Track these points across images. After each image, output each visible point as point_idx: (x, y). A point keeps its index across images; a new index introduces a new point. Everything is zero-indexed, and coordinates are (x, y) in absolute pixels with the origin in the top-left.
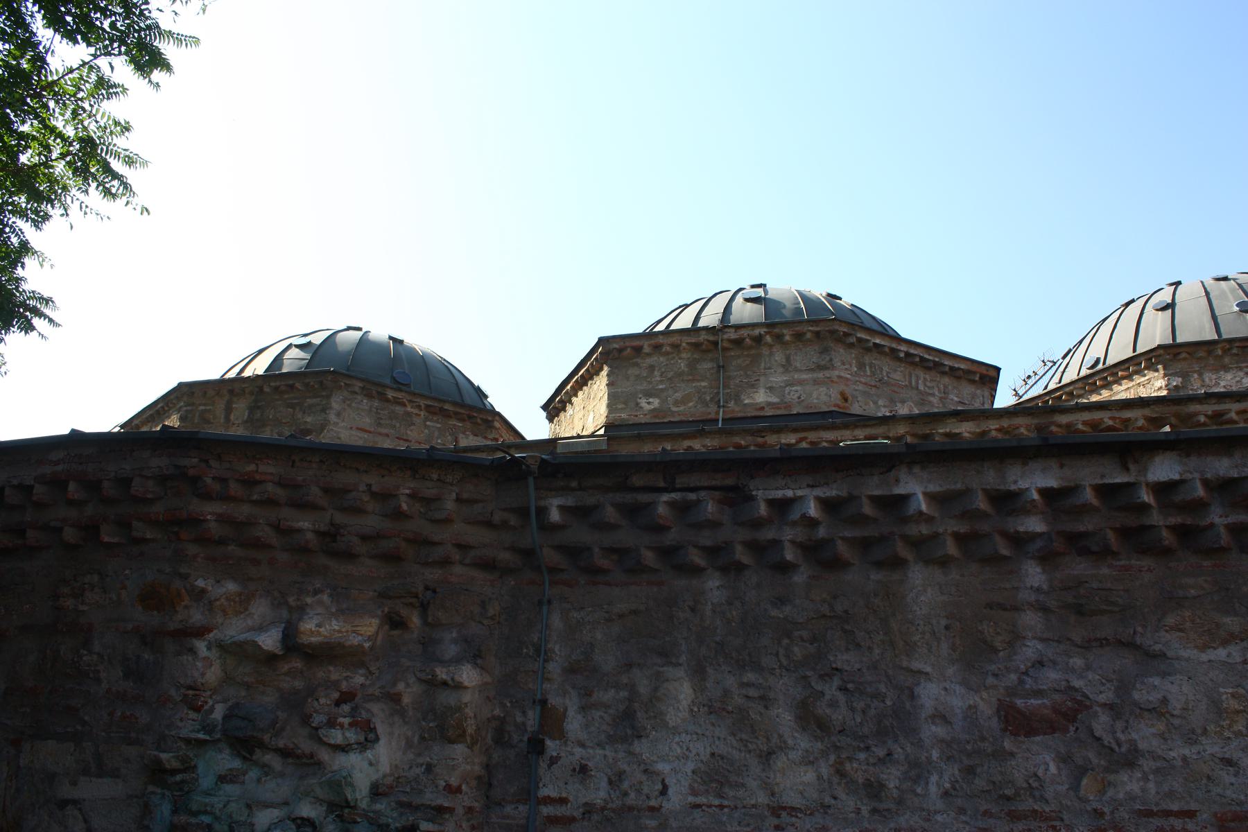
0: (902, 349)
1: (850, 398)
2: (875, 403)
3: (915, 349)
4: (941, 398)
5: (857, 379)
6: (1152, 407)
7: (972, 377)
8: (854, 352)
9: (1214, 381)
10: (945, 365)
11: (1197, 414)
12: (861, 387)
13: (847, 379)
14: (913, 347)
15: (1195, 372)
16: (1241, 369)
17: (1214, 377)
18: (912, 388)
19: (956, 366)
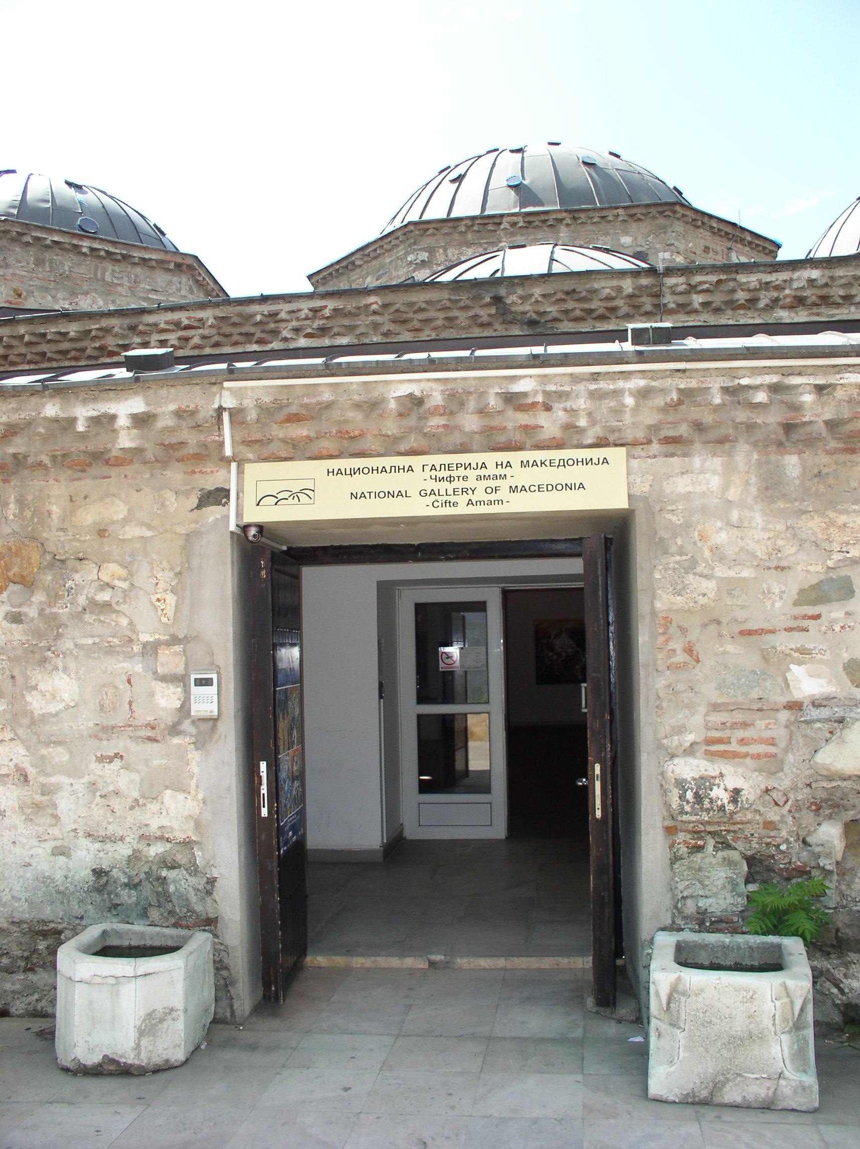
0: (84, 244)
1: (24, 294)
2: (54, 297)
3: (100, 244)
4: (130, 288)
5: (34, 275)
6: (221, 307)
7: (166, 266)
8: (32, 251)
9: (456, 256)
10: (134, 257)
11: (254, 315)
12: (37, 283)
13: (23, 276)
14: (97, 241)
15: (440, 247)
16: (481, 245)
17: (457, 252)
18: (98, 280)
19: (147, 256)
